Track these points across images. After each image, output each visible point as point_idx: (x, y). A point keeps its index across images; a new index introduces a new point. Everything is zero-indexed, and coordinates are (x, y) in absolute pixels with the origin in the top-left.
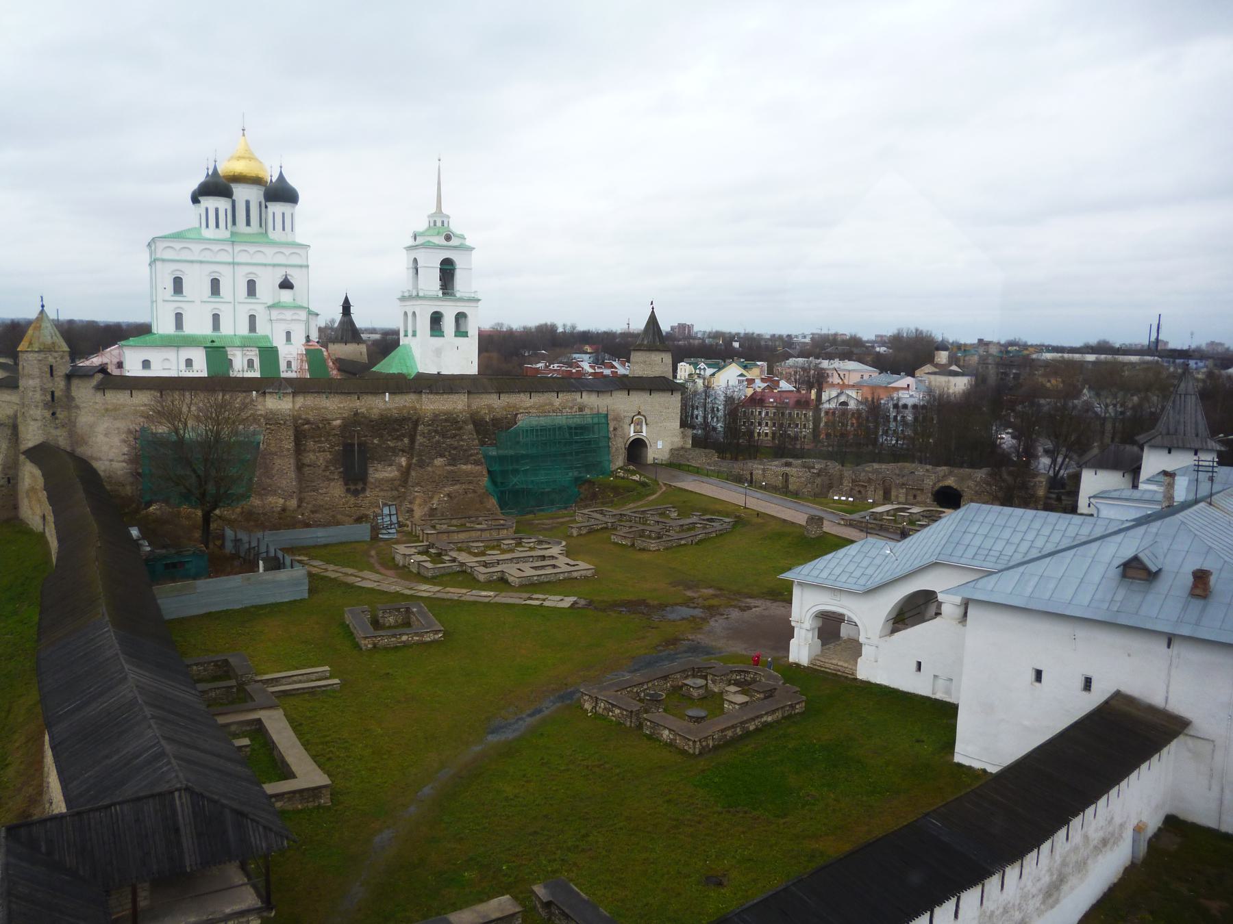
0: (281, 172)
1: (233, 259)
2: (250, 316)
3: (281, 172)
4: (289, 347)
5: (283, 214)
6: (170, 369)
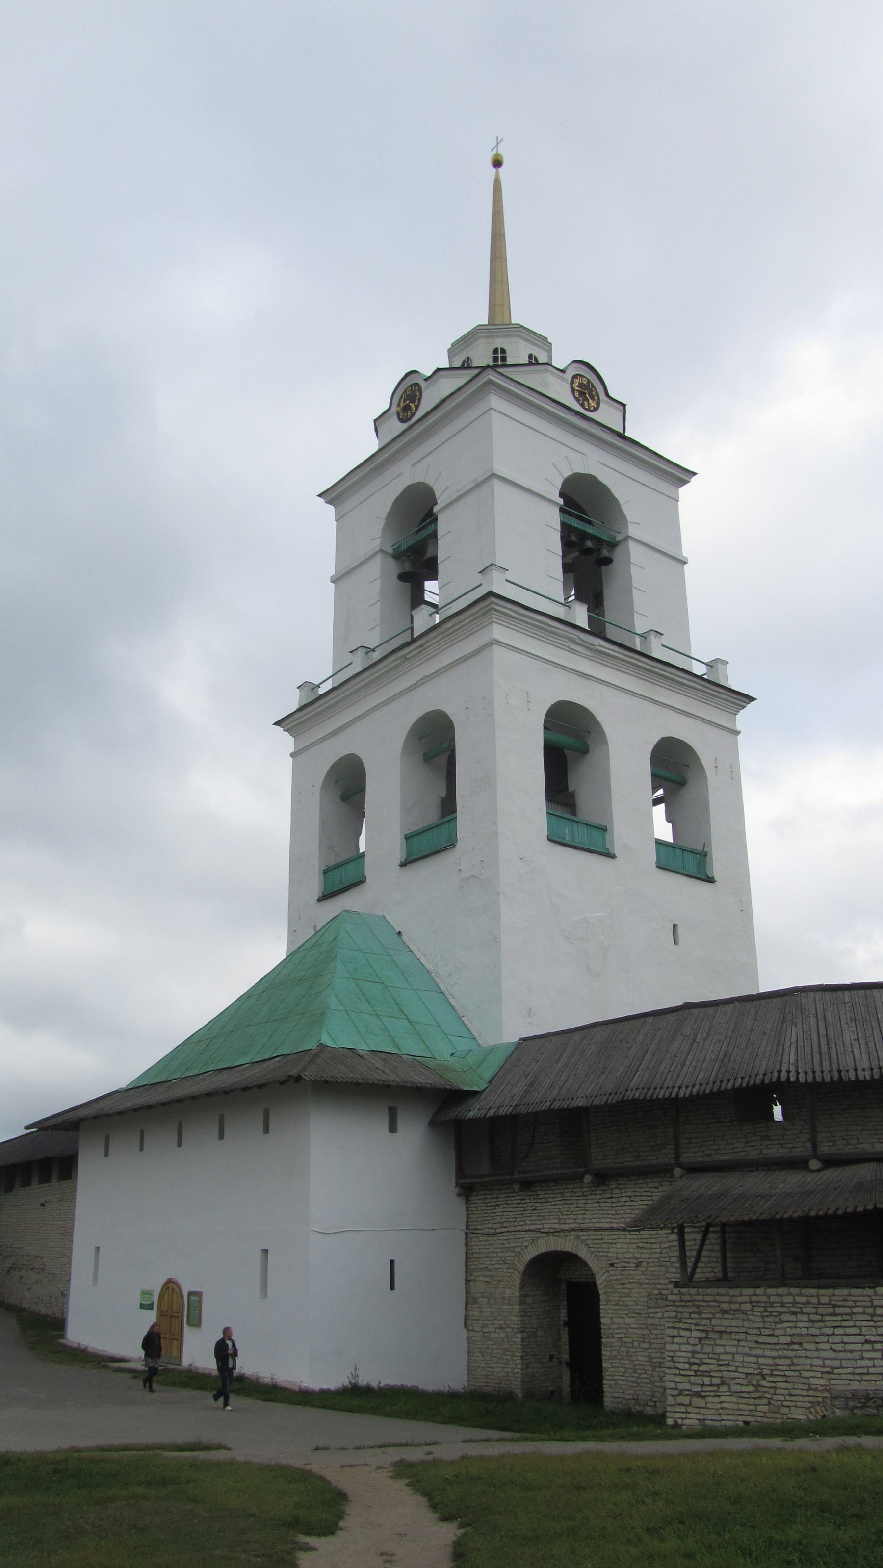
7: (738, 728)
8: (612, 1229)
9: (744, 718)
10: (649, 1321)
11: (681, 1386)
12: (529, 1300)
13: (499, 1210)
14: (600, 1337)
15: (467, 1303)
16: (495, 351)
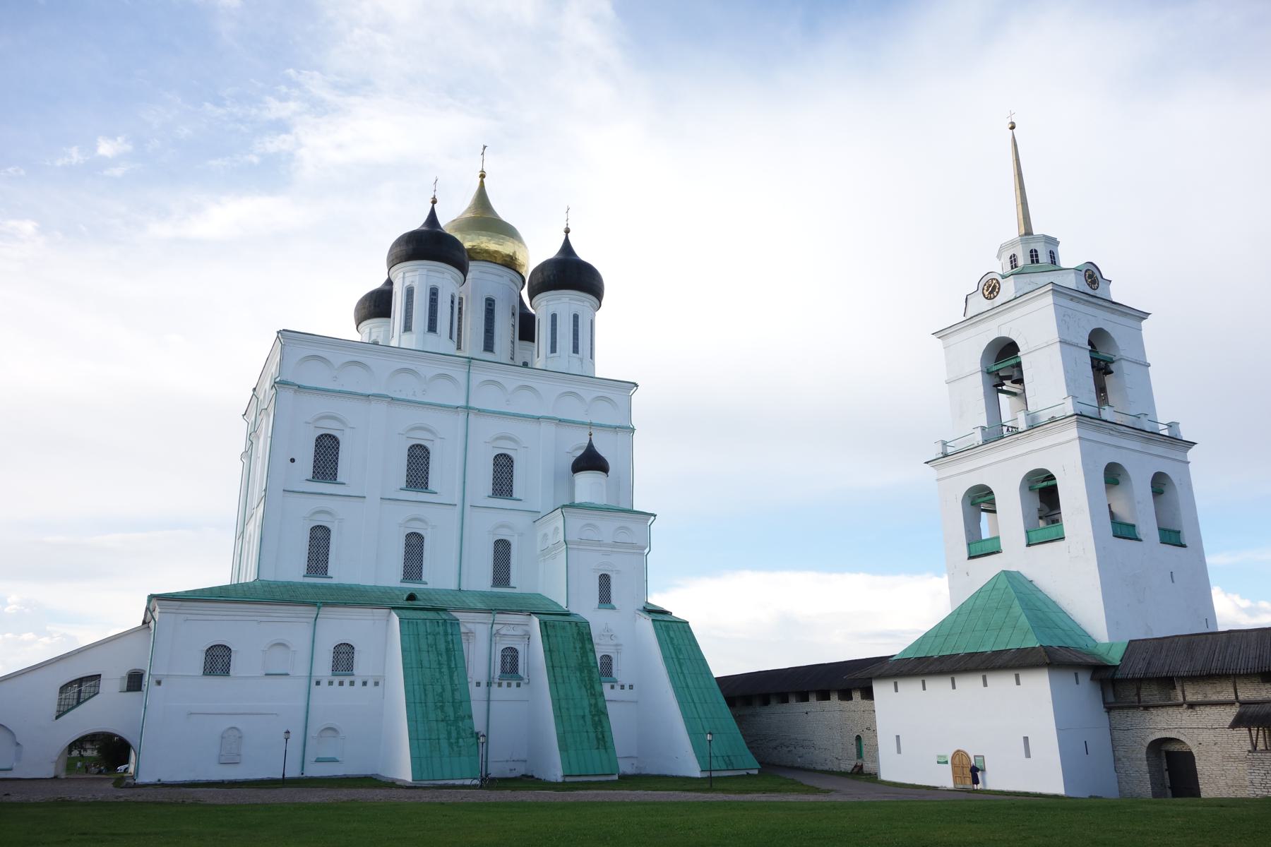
0: (567, 242)
1: (467, 402)
2: (498, 543)
3: (567, 242)
4: (605, 613)
5: (576, 317)
6: (287, 674)
7: (1189, 460)
8: (1198, 728)
9: (1191, 454)
10: (1224, 768)
11: (1257, 793)
12: (1150, 759)
13: (1128, 719)
14: (1197, 775)
15: (1114, 761)
16: (1031, 251)
